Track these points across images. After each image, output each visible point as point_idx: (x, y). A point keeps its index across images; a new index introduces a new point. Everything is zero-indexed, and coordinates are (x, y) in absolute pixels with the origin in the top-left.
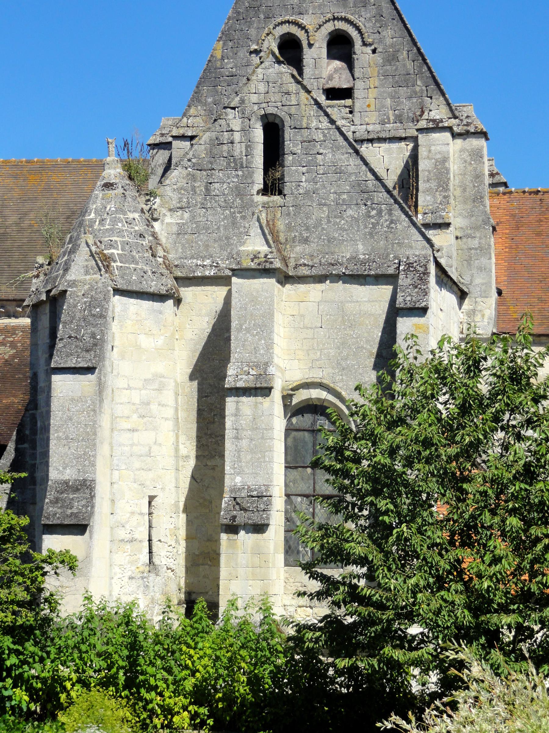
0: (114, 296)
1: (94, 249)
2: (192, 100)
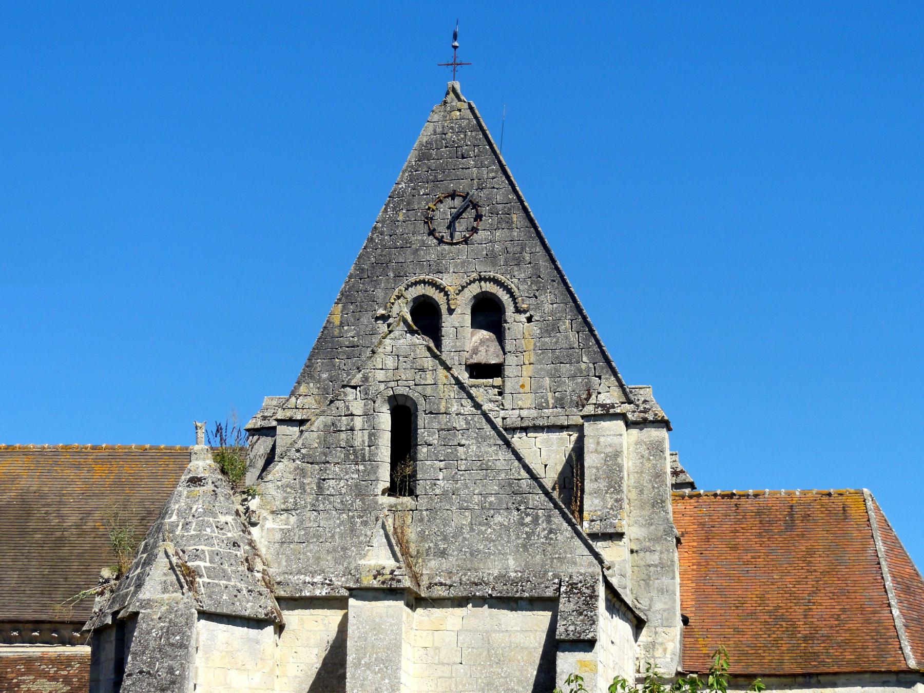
0: (199, 620)
1: (174, 560)
2: (303, 375)
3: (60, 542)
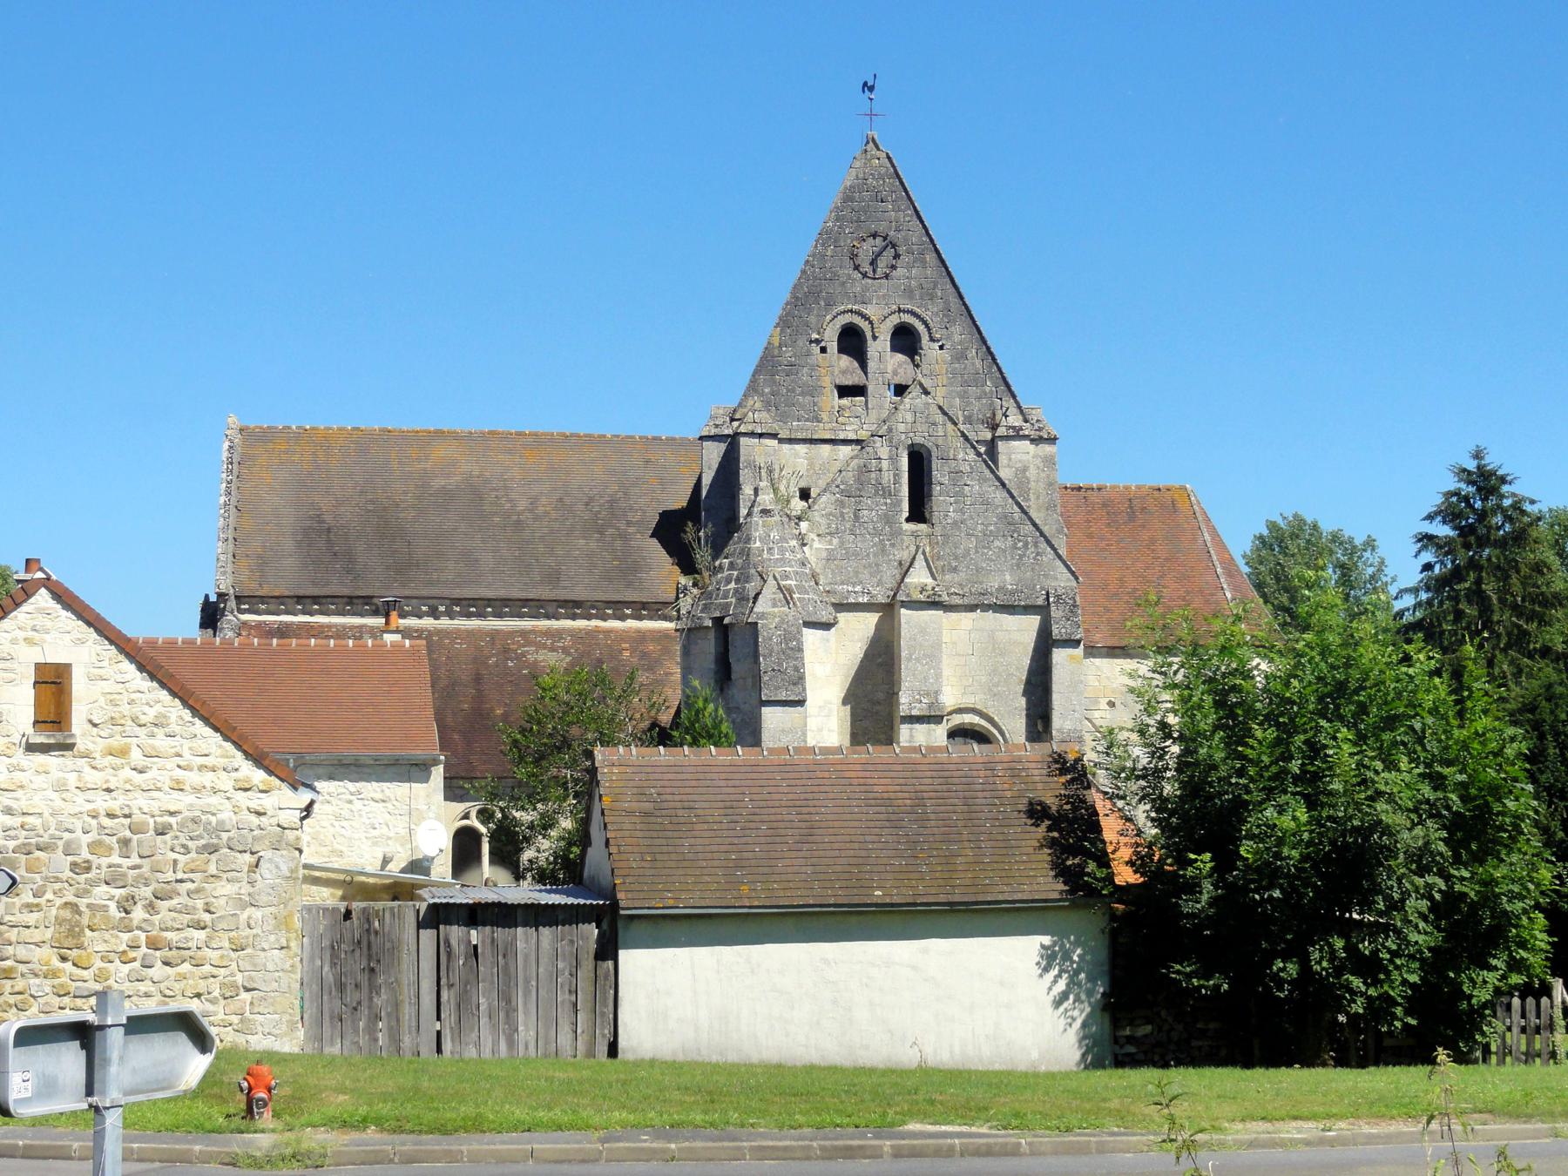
2: (748, 389)
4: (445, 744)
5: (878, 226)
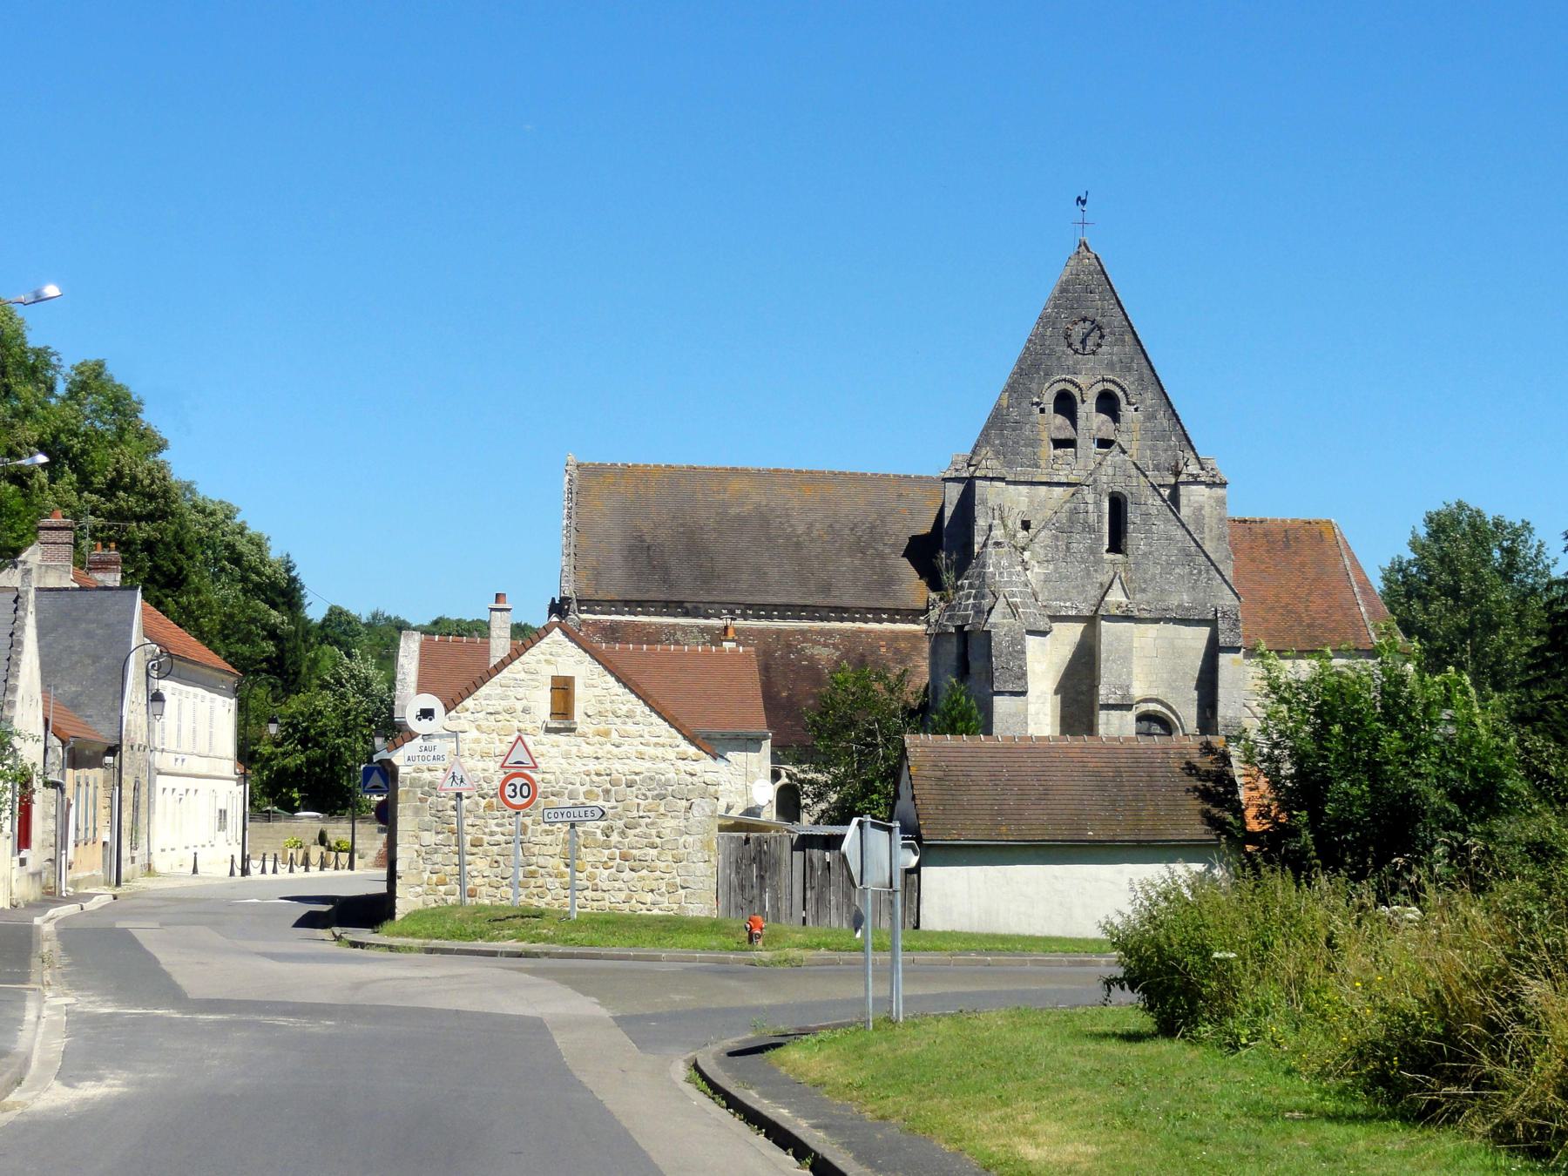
3: (798, 546)
4: (770, 727)
5: (1086, 313)
